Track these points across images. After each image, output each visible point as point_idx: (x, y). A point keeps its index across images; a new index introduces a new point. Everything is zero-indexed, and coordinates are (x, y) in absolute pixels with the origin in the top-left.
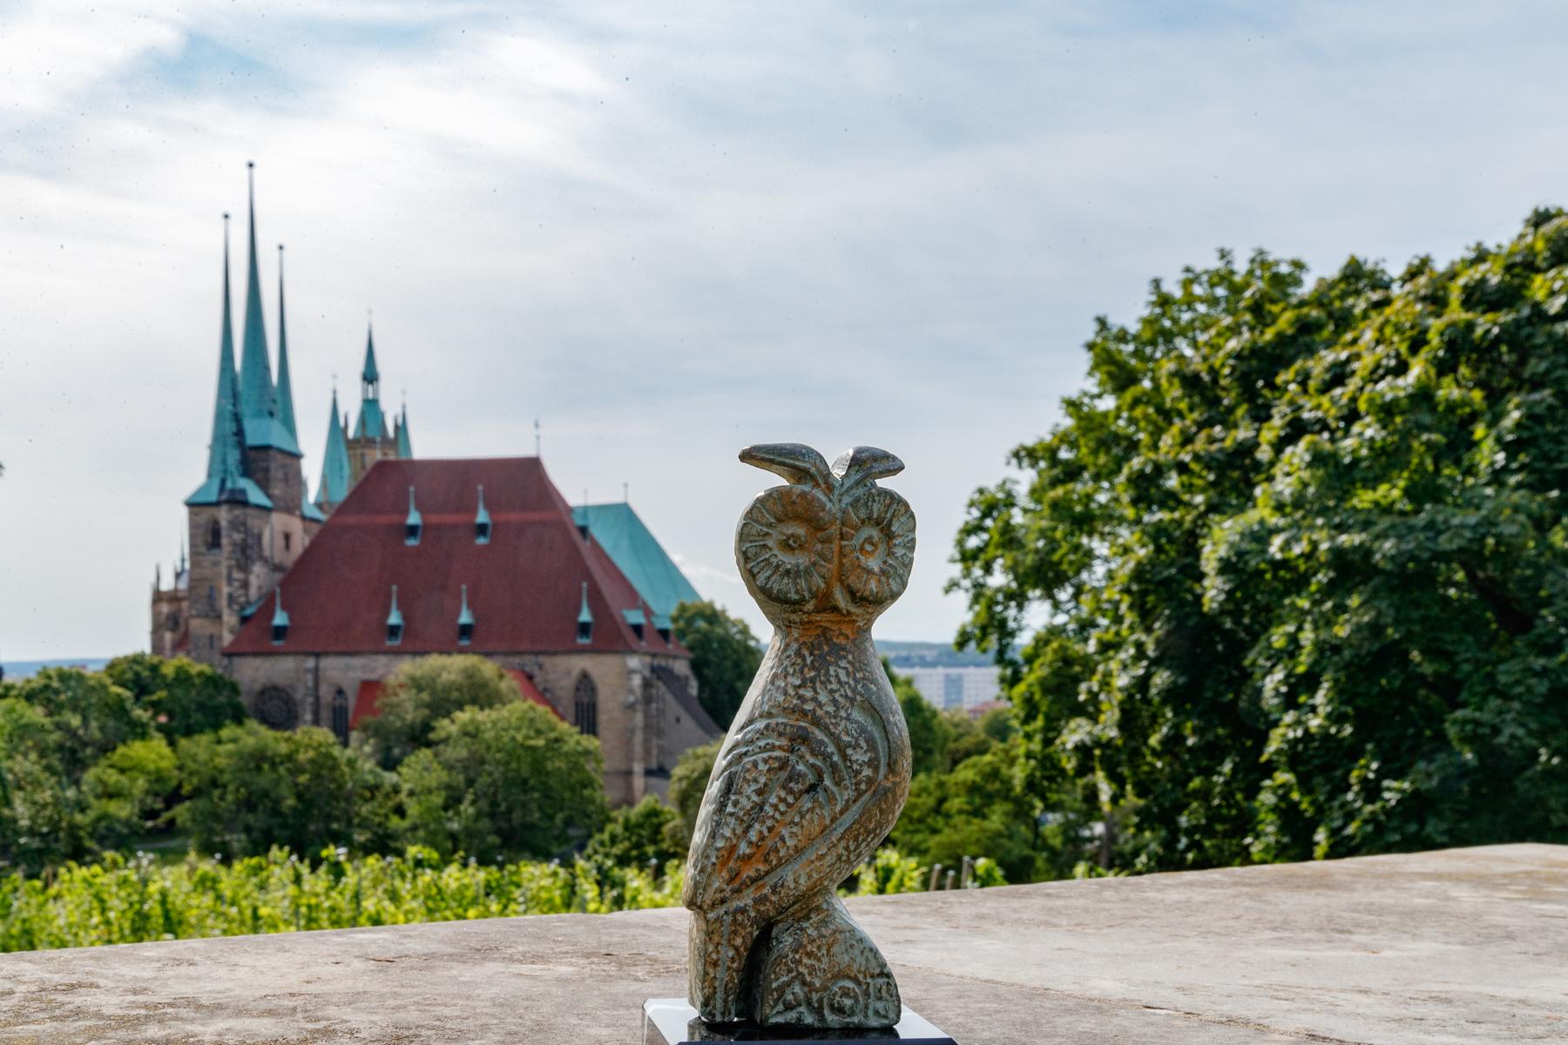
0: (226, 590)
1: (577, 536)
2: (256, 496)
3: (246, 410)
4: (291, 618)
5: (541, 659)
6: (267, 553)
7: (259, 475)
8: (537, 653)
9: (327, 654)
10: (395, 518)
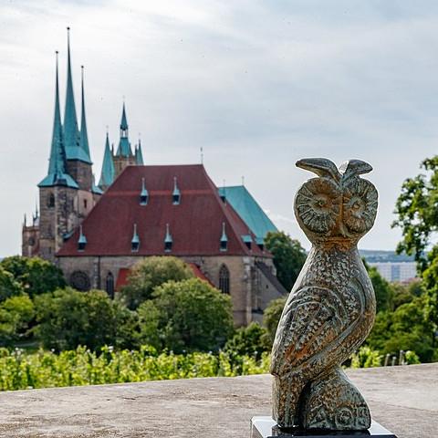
0: (57, 226)
1: (220, 201)
2: (71, 183)
3: (66, 143)
4: (87, 240)
5: (203, 258)
6: (76, 209)
7: (73, 173)
8: (202, 256)
9: (104, 256)
10: (135, 193)
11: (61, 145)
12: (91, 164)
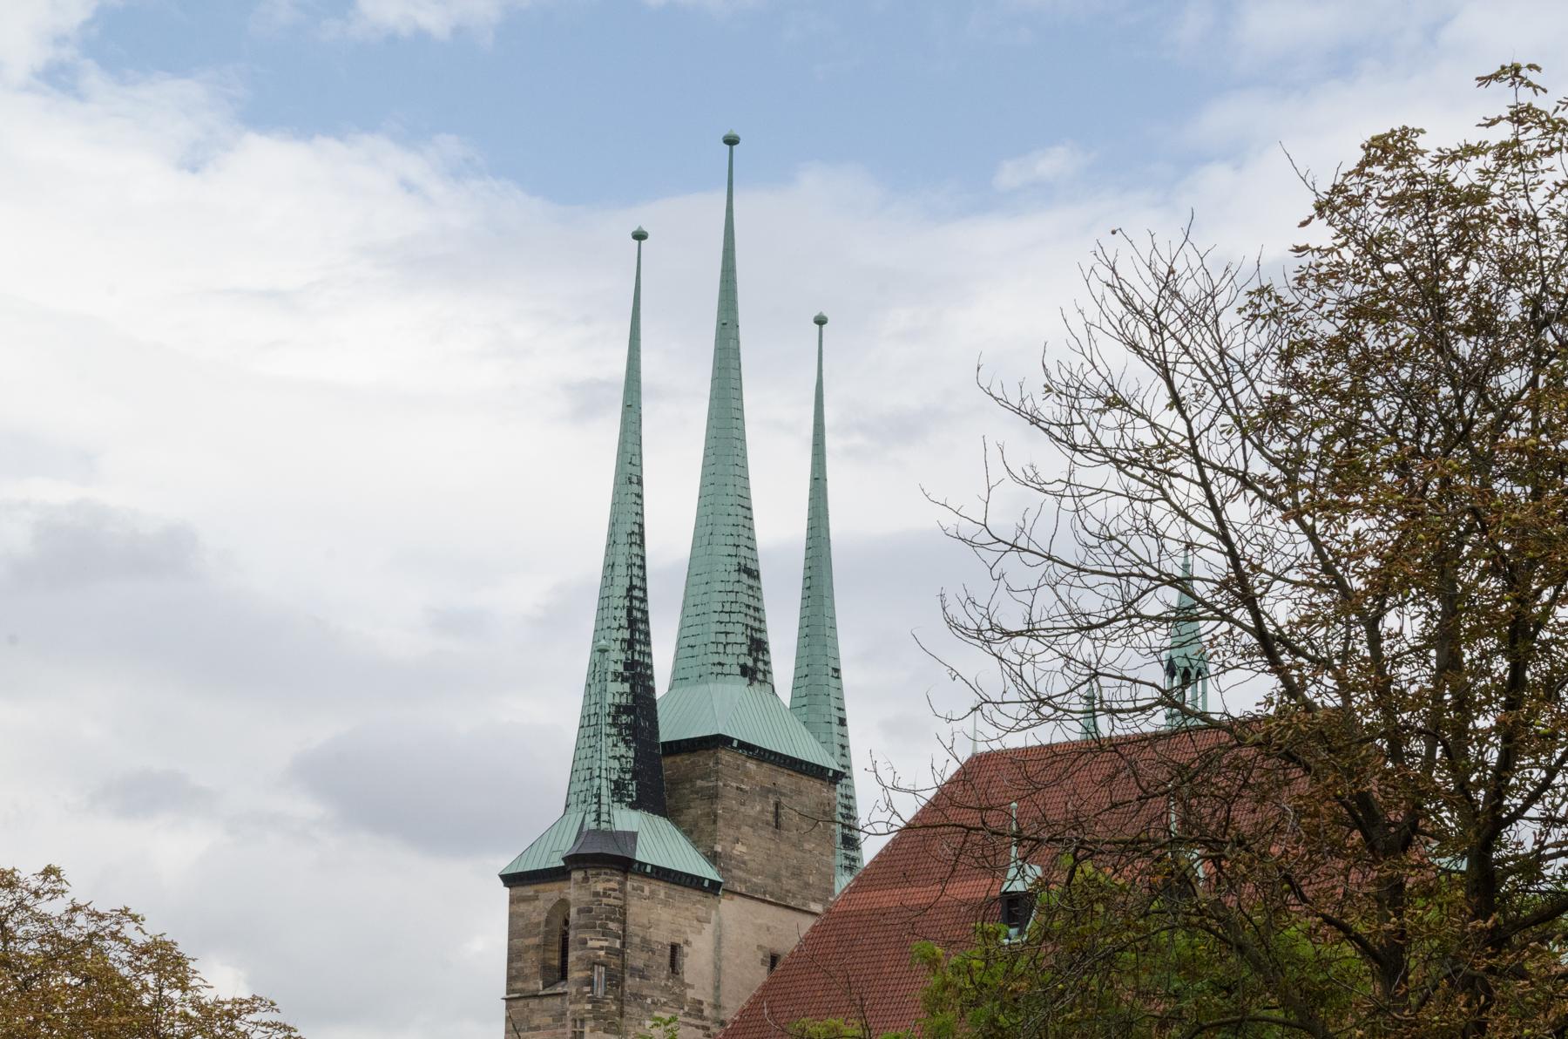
11: (630, 665)
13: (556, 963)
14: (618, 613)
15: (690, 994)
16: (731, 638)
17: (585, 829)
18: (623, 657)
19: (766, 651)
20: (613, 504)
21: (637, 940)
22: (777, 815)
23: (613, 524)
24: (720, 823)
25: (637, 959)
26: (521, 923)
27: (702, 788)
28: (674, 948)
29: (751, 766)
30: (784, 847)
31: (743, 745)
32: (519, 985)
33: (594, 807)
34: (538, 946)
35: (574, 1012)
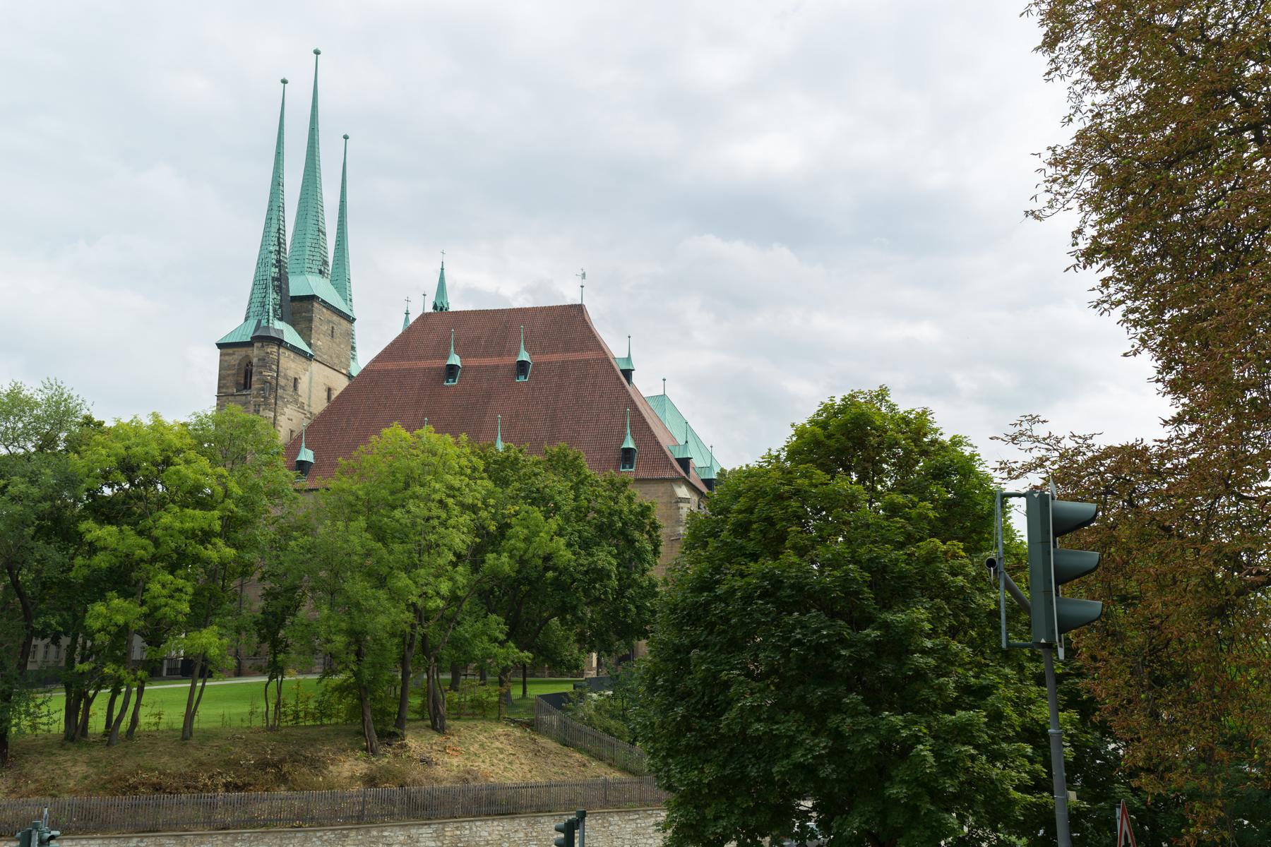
2: (291, 336)
11: (279, 261)
12: (351, 320)
13: (242, 382)
14: (273, 239)
15: (300, 399)
16: (315, 258)
17: (262, 325)
18: (275, 257)
19: (328, 265)
20: (271, 193)
21: (282, 374)
22: (332, 332)
23: (271, 202)
24: (313, 331)
25: (282, 382)
26: (226, 364)
27: (305, 317)
28: (296, 379)
29: (324, 310)
30: (334, 345)
31: (323, 301)
32: (224, 390)
33: (266, 317)
34: (234, 374)
35: (255, 402)
